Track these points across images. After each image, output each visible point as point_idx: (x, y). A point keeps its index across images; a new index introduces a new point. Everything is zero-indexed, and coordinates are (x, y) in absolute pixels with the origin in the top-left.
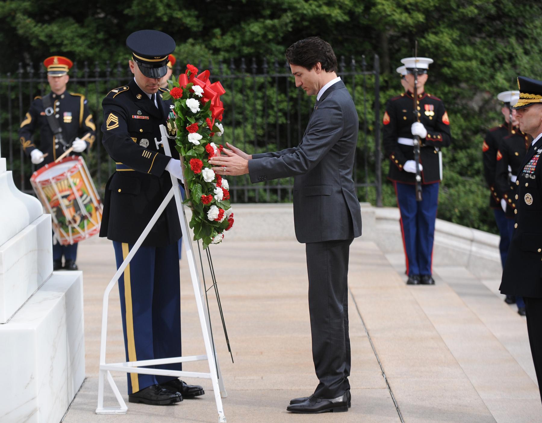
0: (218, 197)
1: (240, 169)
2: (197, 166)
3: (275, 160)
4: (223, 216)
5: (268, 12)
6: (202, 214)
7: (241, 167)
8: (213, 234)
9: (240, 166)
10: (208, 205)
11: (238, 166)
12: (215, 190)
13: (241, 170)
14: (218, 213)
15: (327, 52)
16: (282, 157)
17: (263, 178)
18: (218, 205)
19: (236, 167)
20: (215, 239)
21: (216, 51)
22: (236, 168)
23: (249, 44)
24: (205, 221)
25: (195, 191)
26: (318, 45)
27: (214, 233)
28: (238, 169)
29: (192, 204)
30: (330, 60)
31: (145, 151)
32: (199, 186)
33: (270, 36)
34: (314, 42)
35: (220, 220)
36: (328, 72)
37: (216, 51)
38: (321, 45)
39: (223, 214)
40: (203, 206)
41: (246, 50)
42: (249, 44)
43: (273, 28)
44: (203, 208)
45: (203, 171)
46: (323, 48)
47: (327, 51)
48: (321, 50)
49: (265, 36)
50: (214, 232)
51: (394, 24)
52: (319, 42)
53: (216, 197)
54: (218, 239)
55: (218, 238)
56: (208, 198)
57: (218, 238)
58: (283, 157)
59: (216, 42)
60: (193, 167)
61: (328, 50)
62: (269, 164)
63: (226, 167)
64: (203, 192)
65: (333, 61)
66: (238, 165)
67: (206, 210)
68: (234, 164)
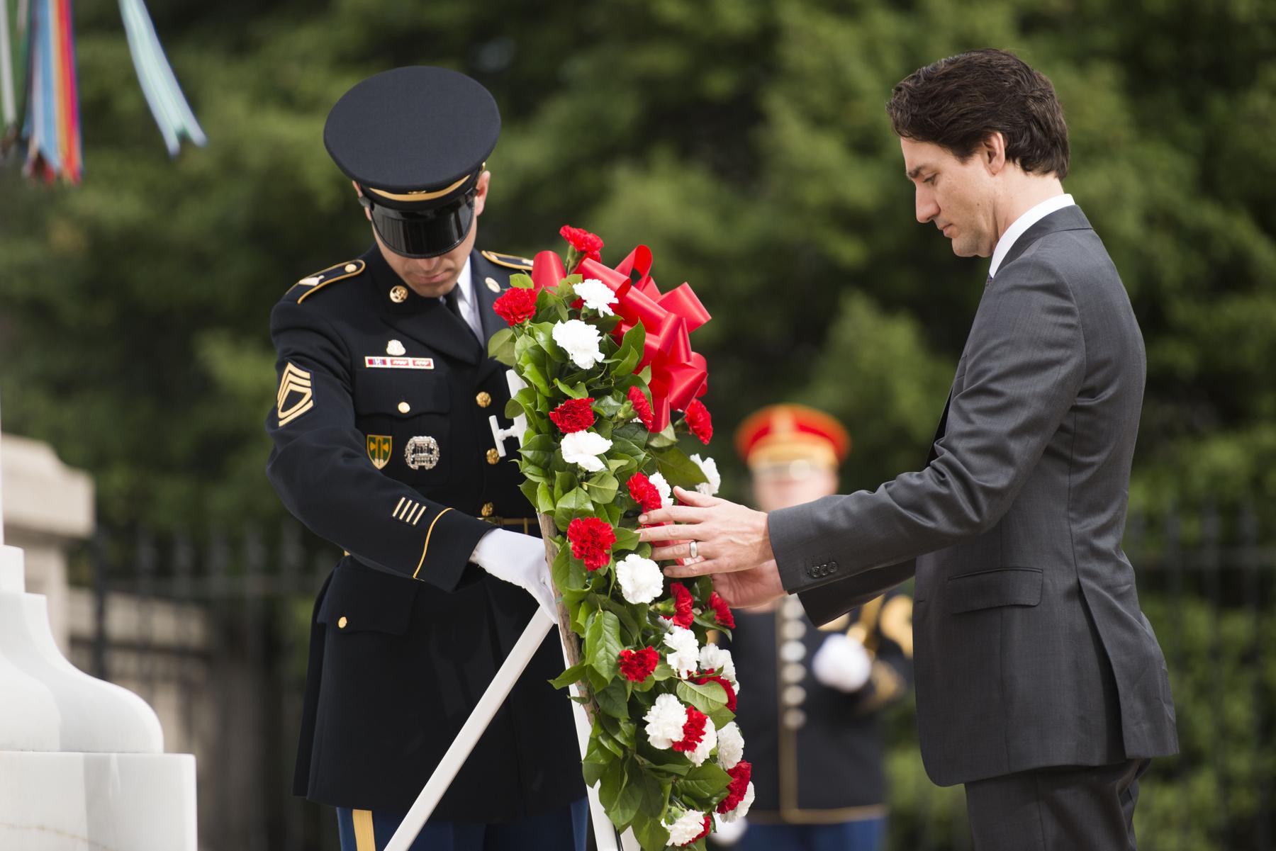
0: (680, 662)
1: (746, 543)
2: (593, 543)
3: (861, 498)
4: (704, 733)
6: (626, 727)
7: (750, 536)
8: (670, 811)
9: (744, 533)
10: (645, 690)
11: (738, 533)
12: (667, 635)
13: (751, 546)
14: (684, 719)
15: (1031, 100)
16: (886, 486)
17: (826, 570)
18: (685, 697)
19: (733, 539)
20: (675, 825)
22: (732, 542)
24: (639, 758)
25: (592, 636)
26: (1001, 73)
27: (674, 809)
28: (738, 545)
29: (588, 692)
30: (1041, 128)
31: (403, 499)
32: (609, 621)
34: (989, 61)
35: (692, 747)
36: (1030, 173)
39: (704, 730)
40: (627, 694)
44: (628, 700)
45: (620, 564)
46: (1018, 82)
48: (1011, 91)
50: (671, 802)
52: (1008, 65)
54: (689, 829)
55: (687, 825)
57: (687, 825)
58: (888, 489)
60: (581, 548)
61: (1038, 93)
62: (840, 514)
63: (696, 541)
65: (1054, 135)
66: (740, 529)
67: (638, 710)
68: (724, 529)
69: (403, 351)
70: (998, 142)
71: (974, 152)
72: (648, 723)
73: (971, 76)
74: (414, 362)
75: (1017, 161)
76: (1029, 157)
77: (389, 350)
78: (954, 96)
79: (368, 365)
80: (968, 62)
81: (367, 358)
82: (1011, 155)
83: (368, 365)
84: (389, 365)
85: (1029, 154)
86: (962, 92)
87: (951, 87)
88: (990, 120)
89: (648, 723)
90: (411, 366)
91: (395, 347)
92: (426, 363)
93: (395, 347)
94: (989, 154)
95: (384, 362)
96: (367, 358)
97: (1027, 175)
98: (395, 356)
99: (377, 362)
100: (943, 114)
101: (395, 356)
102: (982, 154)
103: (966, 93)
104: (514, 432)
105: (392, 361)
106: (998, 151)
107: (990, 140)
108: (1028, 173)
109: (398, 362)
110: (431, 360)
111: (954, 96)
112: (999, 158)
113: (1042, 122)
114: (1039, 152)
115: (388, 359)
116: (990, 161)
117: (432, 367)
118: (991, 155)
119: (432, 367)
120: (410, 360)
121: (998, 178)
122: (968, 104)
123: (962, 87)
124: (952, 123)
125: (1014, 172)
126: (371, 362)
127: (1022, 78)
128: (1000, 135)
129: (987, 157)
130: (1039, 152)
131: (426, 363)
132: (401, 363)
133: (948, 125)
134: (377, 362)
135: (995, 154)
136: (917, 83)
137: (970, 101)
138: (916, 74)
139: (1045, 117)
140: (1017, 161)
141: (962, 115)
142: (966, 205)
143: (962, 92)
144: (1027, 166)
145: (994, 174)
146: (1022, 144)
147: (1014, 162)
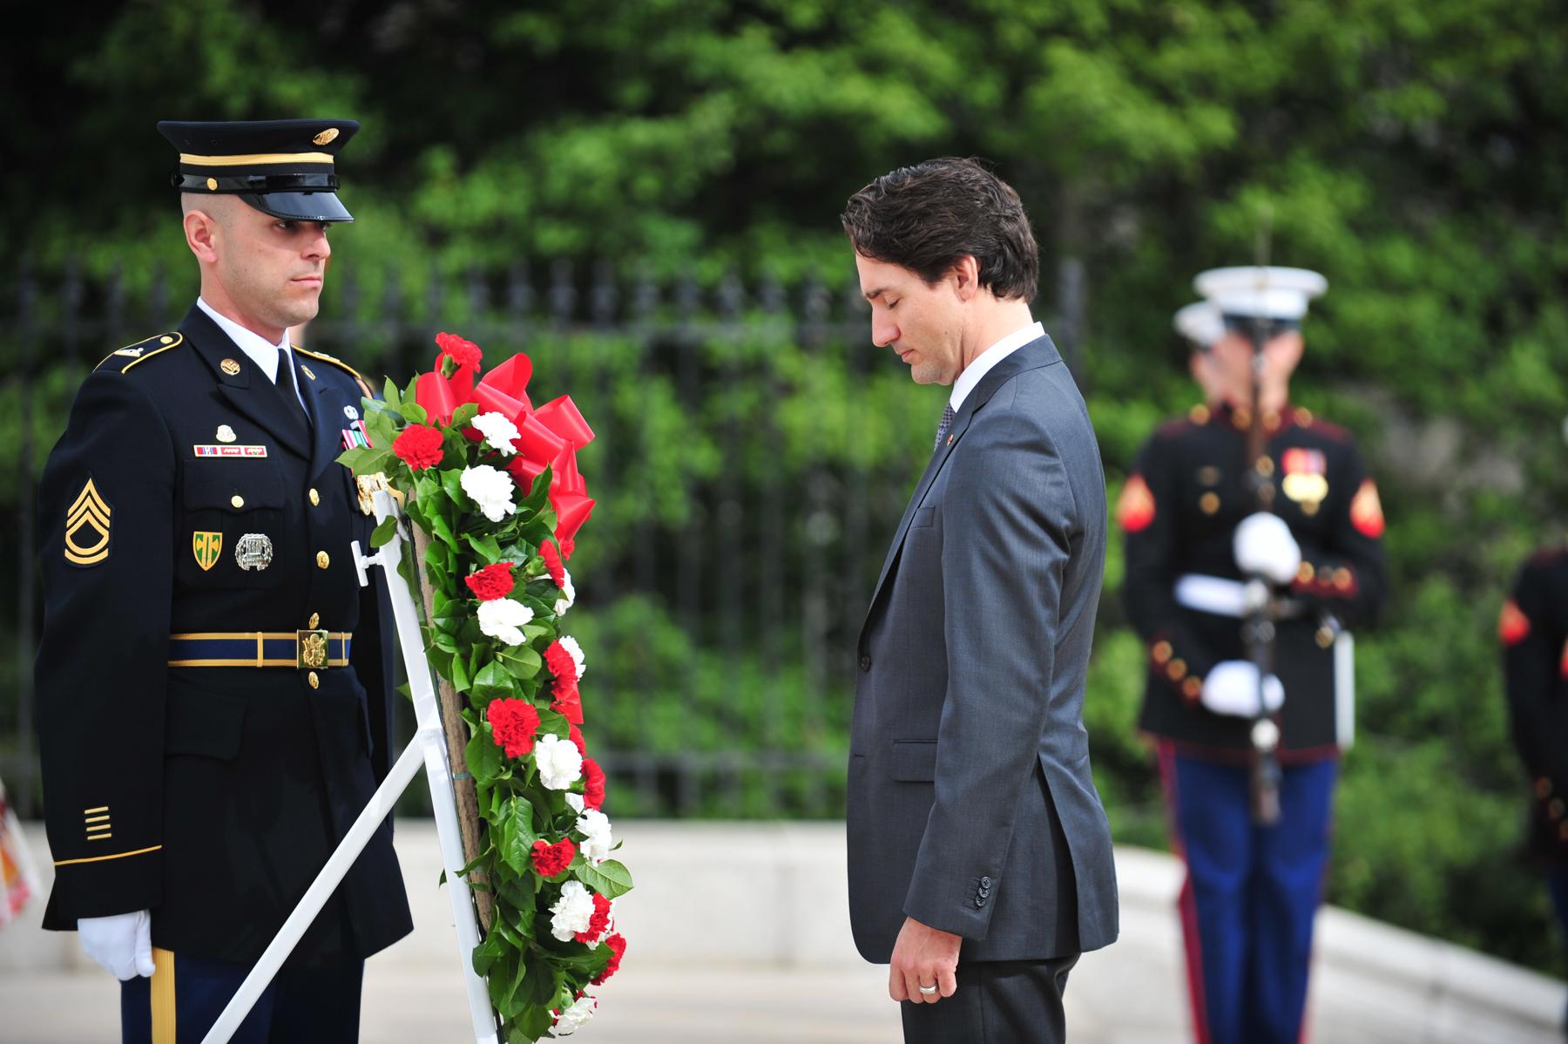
5: (634, 92)
21: (436, 237)
23: (566, 212)
26: (973, 191)
33: (648, 183)
37: (436, 237)
38: (984, 189)
41: (554, 238)
42: (566, 212)
43: (657, 159)
47: (1007, 218)
48: (983, 211)
49: (624, 186)
51: (1114, 151)
53: (585, 848)
56: (560, 852)
59: (437, 202)
64: (536, 828)
69: (233, 437)
70: (971, 266)
71: (945, 277)
72: (553, 914)
73: (941, 194)
74: (246, 450)
75: (989, 286)
76: (1001, 283)
77: (219, 437)
78: (923, 215)
79: (197, 455)
80: (936, 177)
81: (196, 447)
82: (983, 280)
83: (197, 455)
84: (219, 454)
85: (1001, 279)
86: (932, 211)
87: (921, 205)
88: (962, 243)
89: (553, 914)
90: (243, 455)
91: (225, 433)
92: (258, 451)
93: (225, 433)
94: (959, 278)
95: (215, 451)
96: (196, 447)
97: (997, 301)
98: (226, 442)
99: (207, 451)
100: (913, 236)
101: (226, 442)
102: (952, 279)
103: (936, 212)
104: (379, 560)
105: (223, 449)
106: (970, 277)
107: (961, 265)
108: (999, 299)
109: (229, 451)
110: (264, 447)
111: (923, 215)
112: (971, 284)
113: (1016, 245)
114: (1012, 276)
115: (218, 448)
116: (960, 286)
117: (265, 455)
118: (962, 280)
119: (265, 455)
120: (242, 448)
121: (968, 305)
122: (939, 225)
123: (929, 206)
124: (921, 246)
125: (985, 298)
126: (200, 451)
127: (993, 194)
128: (973, 259)
129: (957, 282)
130: (1012, 276)
131: (258, 451)
132: (232, 451)
133: (917, 248)
134: (207, 451)
135: (967, 279)
136: (877, 196)
137: (941, 222)
138: (874, 184)
139: (1019, 238)
140: (989, 286)
141: (933, 238)
142: (934, 335)
143: (932, 211)
144: (999, 290)
145: (964, 300)
146: (995, 269)
147: (985, 287)
